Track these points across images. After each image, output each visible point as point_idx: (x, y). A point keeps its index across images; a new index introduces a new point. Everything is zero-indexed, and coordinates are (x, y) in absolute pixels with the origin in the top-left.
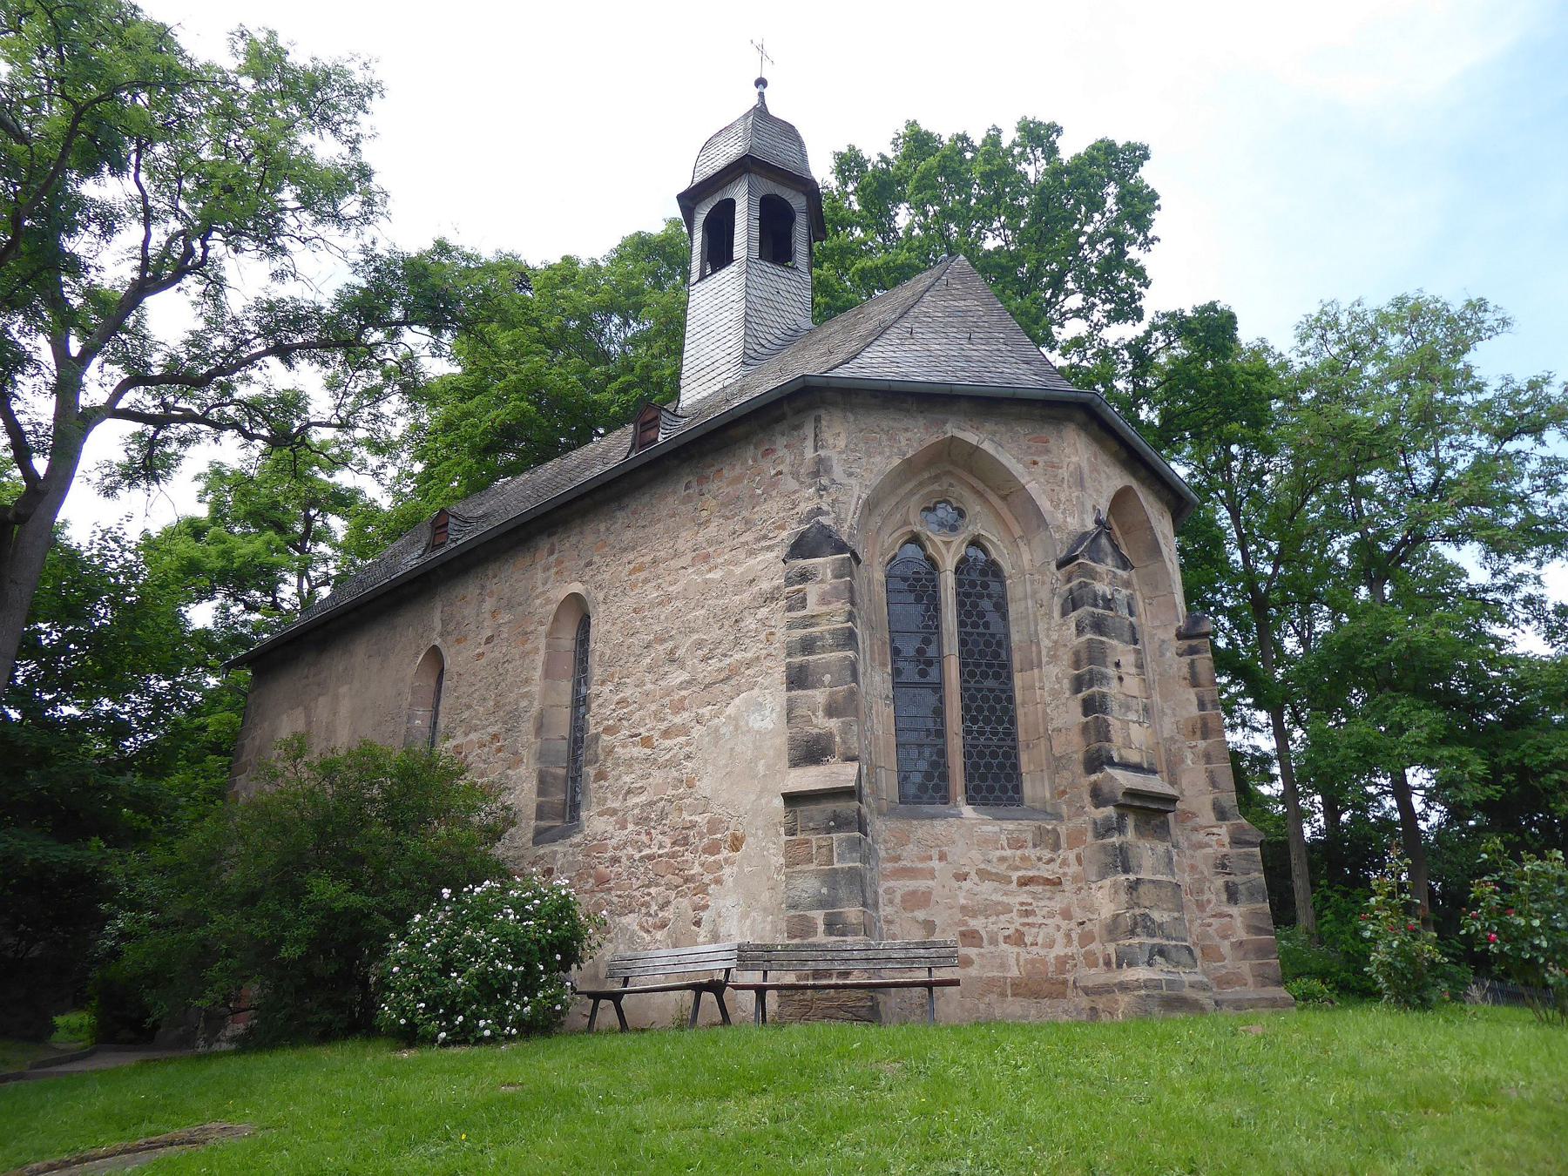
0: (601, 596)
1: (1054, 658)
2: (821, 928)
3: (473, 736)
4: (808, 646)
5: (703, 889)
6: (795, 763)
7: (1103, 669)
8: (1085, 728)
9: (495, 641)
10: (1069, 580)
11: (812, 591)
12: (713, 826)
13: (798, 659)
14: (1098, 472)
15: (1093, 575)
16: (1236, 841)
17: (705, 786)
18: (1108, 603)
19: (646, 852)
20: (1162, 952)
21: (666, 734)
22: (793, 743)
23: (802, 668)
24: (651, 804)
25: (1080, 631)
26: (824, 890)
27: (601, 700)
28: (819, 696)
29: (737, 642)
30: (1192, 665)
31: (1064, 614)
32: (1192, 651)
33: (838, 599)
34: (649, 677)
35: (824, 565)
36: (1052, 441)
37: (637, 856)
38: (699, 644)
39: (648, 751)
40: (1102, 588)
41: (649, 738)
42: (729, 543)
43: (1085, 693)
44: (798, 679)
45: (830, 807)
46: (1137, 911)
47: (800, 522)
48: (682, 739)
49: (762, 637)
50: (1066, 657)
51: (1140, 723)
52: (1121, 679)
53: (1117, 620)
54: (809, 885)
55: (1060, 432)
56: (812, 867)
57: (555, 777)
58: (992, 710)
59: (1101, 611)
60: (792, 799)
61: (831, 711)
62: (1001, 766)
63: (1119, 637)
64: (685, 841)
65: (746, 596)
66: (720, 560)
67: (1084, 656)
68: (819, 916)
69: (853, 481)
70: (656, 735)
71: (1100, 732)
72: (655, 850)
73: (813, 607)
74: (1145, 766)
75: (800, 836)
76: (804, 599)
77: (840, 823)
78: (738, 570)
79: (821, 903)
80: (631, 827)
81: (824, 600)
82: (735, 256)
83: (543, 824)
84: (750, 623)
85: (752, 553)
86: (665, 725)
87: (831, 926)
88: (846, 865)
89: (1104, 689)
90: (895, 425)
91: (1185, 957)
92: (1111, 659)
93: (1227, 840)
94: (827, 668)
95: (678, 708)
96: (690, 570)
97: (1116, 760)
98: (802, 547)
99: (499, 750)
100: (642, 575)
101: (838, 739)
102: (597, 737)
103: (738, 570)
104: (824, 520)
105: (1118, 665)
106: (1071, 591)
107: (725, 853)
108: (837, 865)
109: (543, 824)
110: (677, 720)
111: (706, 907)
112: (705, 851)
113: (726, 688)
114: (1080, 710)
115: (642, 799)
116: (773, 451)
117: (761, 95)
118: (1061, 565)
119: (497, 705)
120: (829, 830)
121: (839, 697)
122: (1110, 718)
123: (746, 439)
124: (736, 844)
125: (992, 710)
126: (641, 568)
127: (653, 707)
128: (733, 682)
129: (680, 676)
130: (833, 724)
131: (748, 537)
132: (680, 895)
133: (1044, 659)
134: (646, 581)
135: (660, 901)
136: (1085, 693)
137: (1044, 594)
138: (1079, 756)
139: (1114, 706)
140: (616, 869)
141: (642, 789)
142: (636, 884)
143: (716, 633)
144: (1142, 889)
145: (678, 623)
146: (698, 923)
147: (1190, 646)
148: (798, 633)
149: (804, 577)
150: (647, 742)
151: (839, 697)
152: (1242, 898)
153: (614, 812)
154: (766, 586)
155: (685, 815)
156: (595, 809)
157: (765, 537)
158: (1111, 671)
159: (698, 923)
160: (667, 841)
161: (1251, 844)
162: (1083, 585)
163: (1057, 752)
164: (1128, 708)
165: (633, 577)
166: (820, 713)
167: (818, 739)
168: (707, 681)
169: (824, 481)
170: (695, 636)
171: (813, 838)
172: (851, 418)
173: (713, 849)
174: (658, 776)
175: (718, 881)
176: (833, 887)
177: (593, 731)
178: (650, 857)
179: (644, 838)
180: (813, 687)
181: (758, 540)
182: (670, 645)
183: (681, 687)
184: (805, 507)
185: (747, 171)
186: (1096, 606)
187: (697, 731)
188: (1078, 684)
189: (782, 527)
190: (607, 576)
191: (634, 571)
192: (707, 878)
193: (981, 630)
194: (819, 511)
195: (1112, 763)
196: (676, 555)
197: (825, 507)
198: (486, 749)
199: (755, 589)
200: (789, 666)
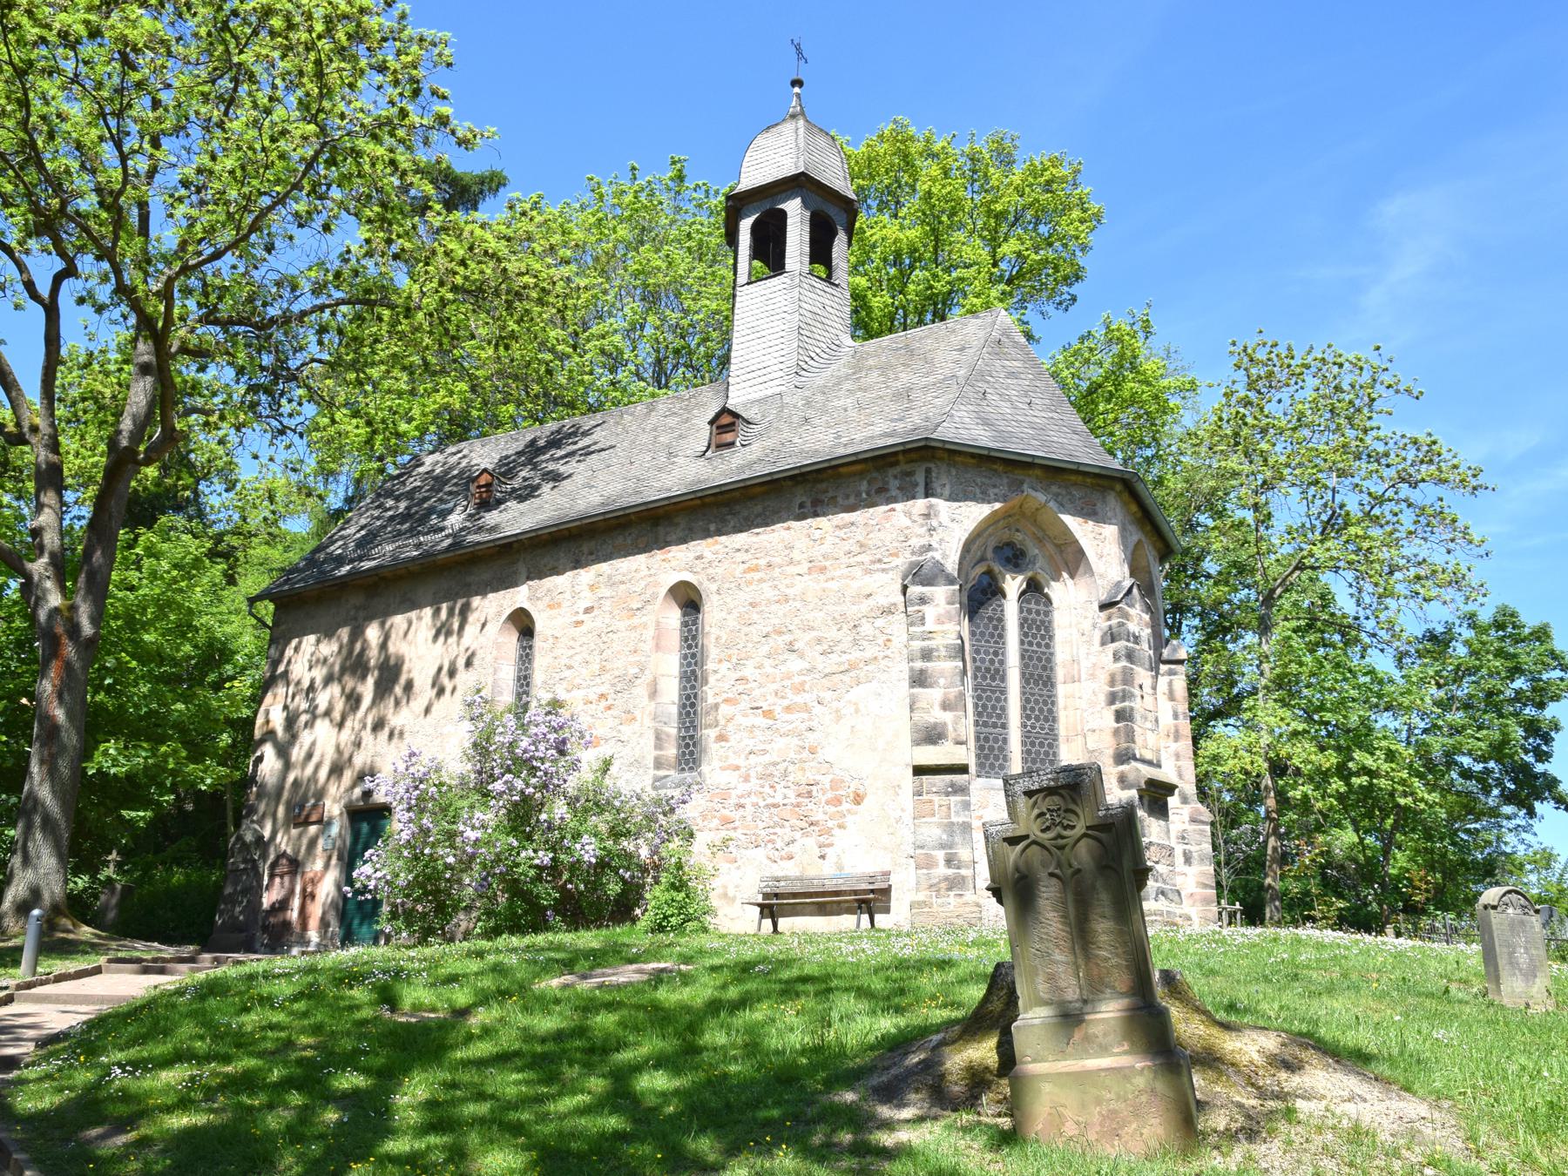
0: (714, 587)
1: (1093, 676)
2: (942, 862)
4: (927, 655)
5: (828, 832)
6: (917, 743)
8: (1116, 732)
9: (596, 612)
10: (1109, 618)
12: (835, 785)
13: (919, 665)
15: (1126, 616)
16: (1193, 820)
17: (827, 753)
19: (770, 801)
20: (1163, 893)
21: (788, 709)
22: (916, 728)
23: (922, 672)
24: (775, 764)
25: (1116, 658)
26: (944, 837)
27: (718, 676)
29: (855, 642)
30: (1170, 684)
31: (1103, 644)
33: (950, 620)
34: (767, 663)
37: (762, 804)
38: (819, 641)
39: (771, 722)
41: (770, 711)
42: (845, 560)
43: (1118, 706)
44: (920, 680)
45: (948, 778)
47: (913, 553)
48: (805, 715)
49: (881, 641)
50: (1103, 678)
54: (932, 832)
56: (935, 819)
57: (668, 735)
58: (1041, 710)
60: (919, 771)
61: (945, 706)
62: (1047, 754)
63: (1142, 665)
64: (810, 795)
65: (865, 606)
66: (837, 573)
67: (1119, 678)
68: (940, 855)
69: (954, 525)
70: (778, 709)
72: (778, 799)
73: (929, 625)
75: (925, 797)
76: (923, 618)
78: (855, 585)
79: (942, 846)
80: (754, 781)
81: (939, 621)
82: (787, 267)
83: (662, 773)
84: (866, 629)
85: (868, 572)
86: (786, 703)
87: (949, 862)
88: (961, 820)
90: (987, 481)
91: (1176, 898)
92: (1137, 682)
93: (1187, 819)
94: (942, 674)
95: (800, 689)
96: (806, 577)
99: (609, 708)
100: (757, 576)
101: (950, 728)
102: (716, 706)
103: (855, 585)
106: (1110, 628)
107: (845, 806)
108: (954, 819)
109: (662, 773)
110: (799, 699)
111: (830, 845)
112: (828, 803)
113: (846, 678)
114: (1112, 718)
115: (767, 759)
116: (887, 490)
118: (1104, 607)
119: (603, 669)
120: (947, 794)
121: (952, 697)
124: (858, 799)
125: (1041, 710)
126: (756, 569)
127: (775, 687)
128: (852, 674)
129: (795, 664)
131: (865, 558)
132: (806, 835)
133: (1083, 677)
134: (761, 581)
135: (787, 839)
136: (1118, 706)
137: (1087, 625)
138: (1111, 752)
139: (1137, 716)
140: (741, 811)
141: (765, 752)
142: (761, 825)
143: (833, 634)
145: (796, 620)
146: (823, 857)
148: (917, 645)
150: (768, 714)
151: (952, 697)
152: (1195, 861)
153: (737, 768)
154: (884, 602)
155: (808, 774)
156: (716, 763)
157: (880, 561)
158: (1137, 692)
159: (823, 857)
160: (791, 794)
161: (1203, 823)
162: (1121, 625)
163: (1091, 746)
165: (749, 576)
166: (937, 707)
167: (935, 726)
168: (827, 671)
169: (935, 523)
170: (814, 634)
171: (936, 798)
172: (954, 472)
173: (837, 801)
174: (780, 743)
175: (841, 826)
176: (951, 834)
177: (711, 700)
178: (775, 806)
179: (767, 790)
180: (931, 686)
181: (873, 562)
182: (788, 638)
183: (800, 673)
184: (916, 542)
185: (801, 187)
187: (818, 709)
188: (1112, 698)
189: (896, 555)
190: (720, 571)
191: (750, 570)
192: (830, 824)
193: (1035, 648)
194: (929, 548)
195: (1135, 759)
196: (791, 562)
197: (935, 545)
198: (593, 706)
199: (871, 602)
200: (912, 669)
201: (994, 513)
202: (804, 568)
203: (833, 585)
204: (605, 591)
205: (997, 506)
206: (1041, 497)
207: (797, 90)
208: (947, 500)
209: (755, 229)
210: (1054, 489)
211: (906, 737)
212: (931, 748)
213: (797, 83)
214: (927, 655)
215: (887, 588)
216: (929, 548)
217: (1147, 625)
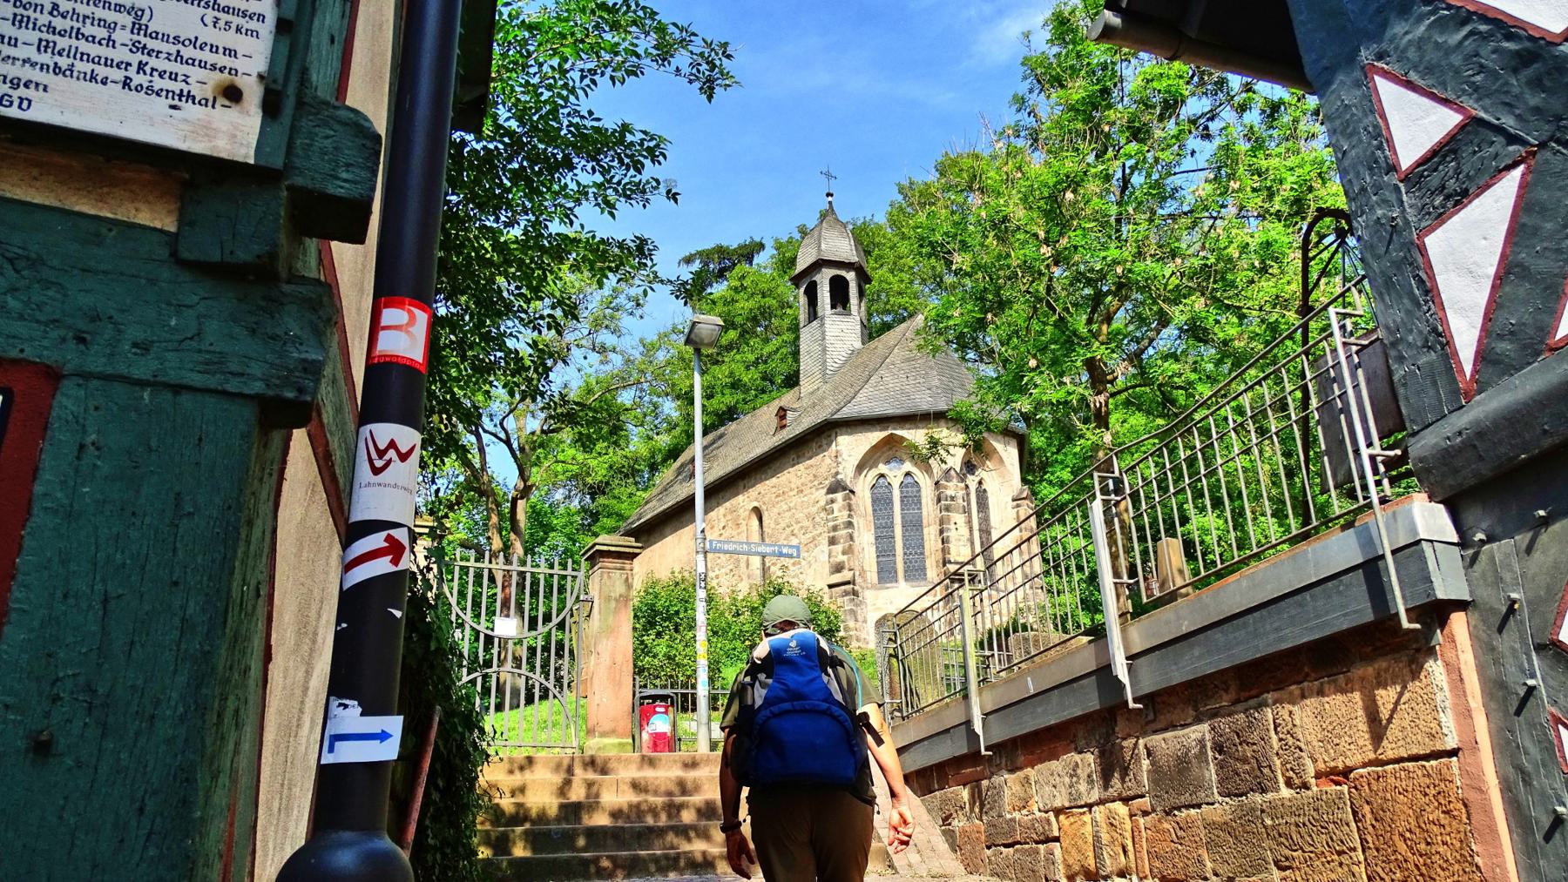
3: (723, 570)
4: (835, 528)
6: (832, 573)
11: (836, 506)
13: (832, 534)
18: (953, 498)
22: (831, 567)
28: (839, 548)
32: (1018, 506)
35: (839, 496)
40: (950, 492)
44: (832, 542)
45: (843, 588)
60: (831, 586)
61: (844, 553)
63: (958, 512)
71: (945, 551)
73: (836, 514)
77: (846, 593)
98: (832, 490)
104: (839, 477)
117: (830, 203)
123: (812, 440)
130: (845, 558)
131: (816, 483)
148: (831, 524)
149: (832, 501)
194: (837, 473)
202: (795, 492)
203: (806, 499)
204: (729, 517)
207: (830, 199)
209: (805, 292)
211: (827, 570)
212: (838, 575)
213: (829, 195)
214: (835, 528)
215: (821, 496)
216: (837, 473)
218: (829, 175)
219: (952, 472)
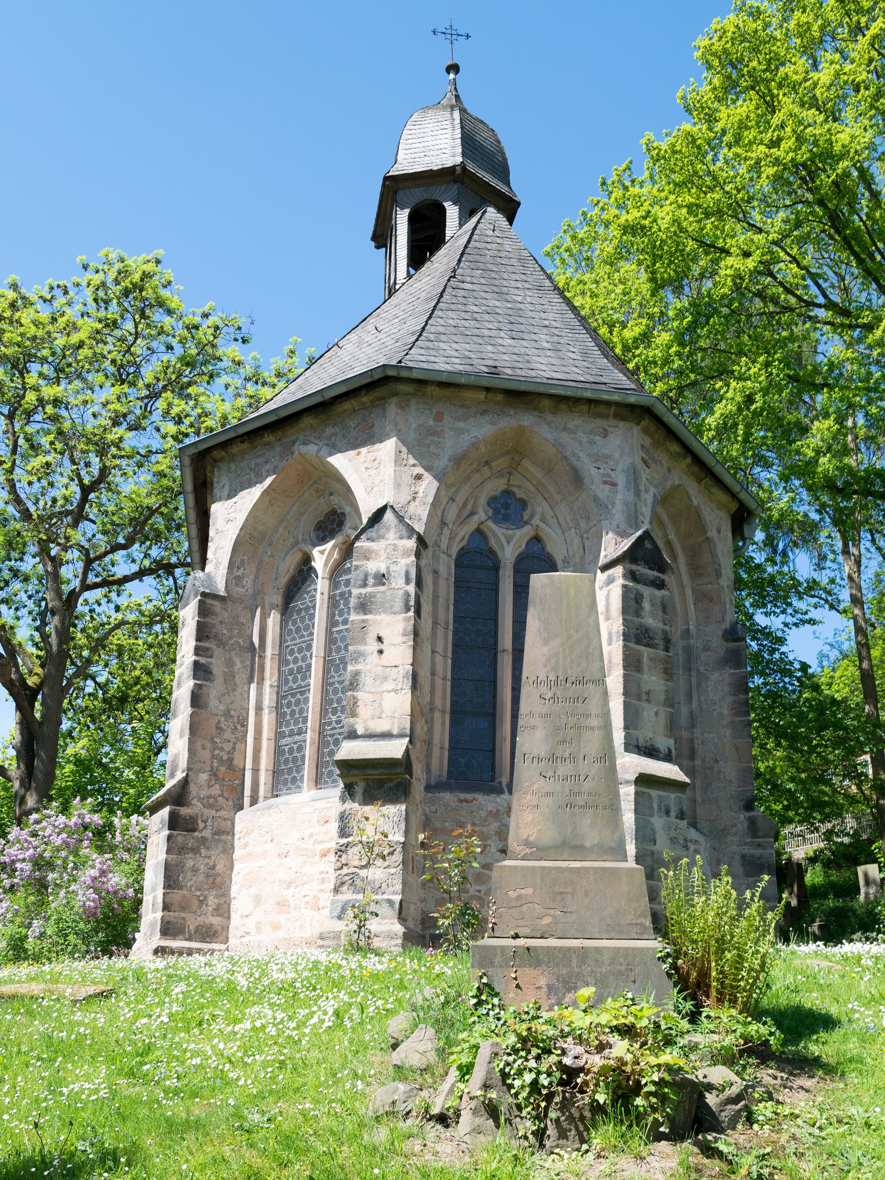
7: (361, 648)
14: (439, 434)
36: (377, 423)
46: (345, 871)
51: (396, 691)
52: (381, 652)
53: (389, 593)
55: (384, 411)
59: (368, 590)
74: (395, 732)
89: (359, 667)
90: (260, 460)
97: (360, 732)
105: (380, 639)
122: (360, 695)
144: (351, 851)
147: (609, 576)
164: (385, 678)
186: (365, 585)
201: (265, 493)
205: (268, 481)
206: (312, 449)
208: (230, 497)
210: (329, 431)
213: (453, 68)
217: (406, 554)
218: (451, 34)
219: (389, 516)
